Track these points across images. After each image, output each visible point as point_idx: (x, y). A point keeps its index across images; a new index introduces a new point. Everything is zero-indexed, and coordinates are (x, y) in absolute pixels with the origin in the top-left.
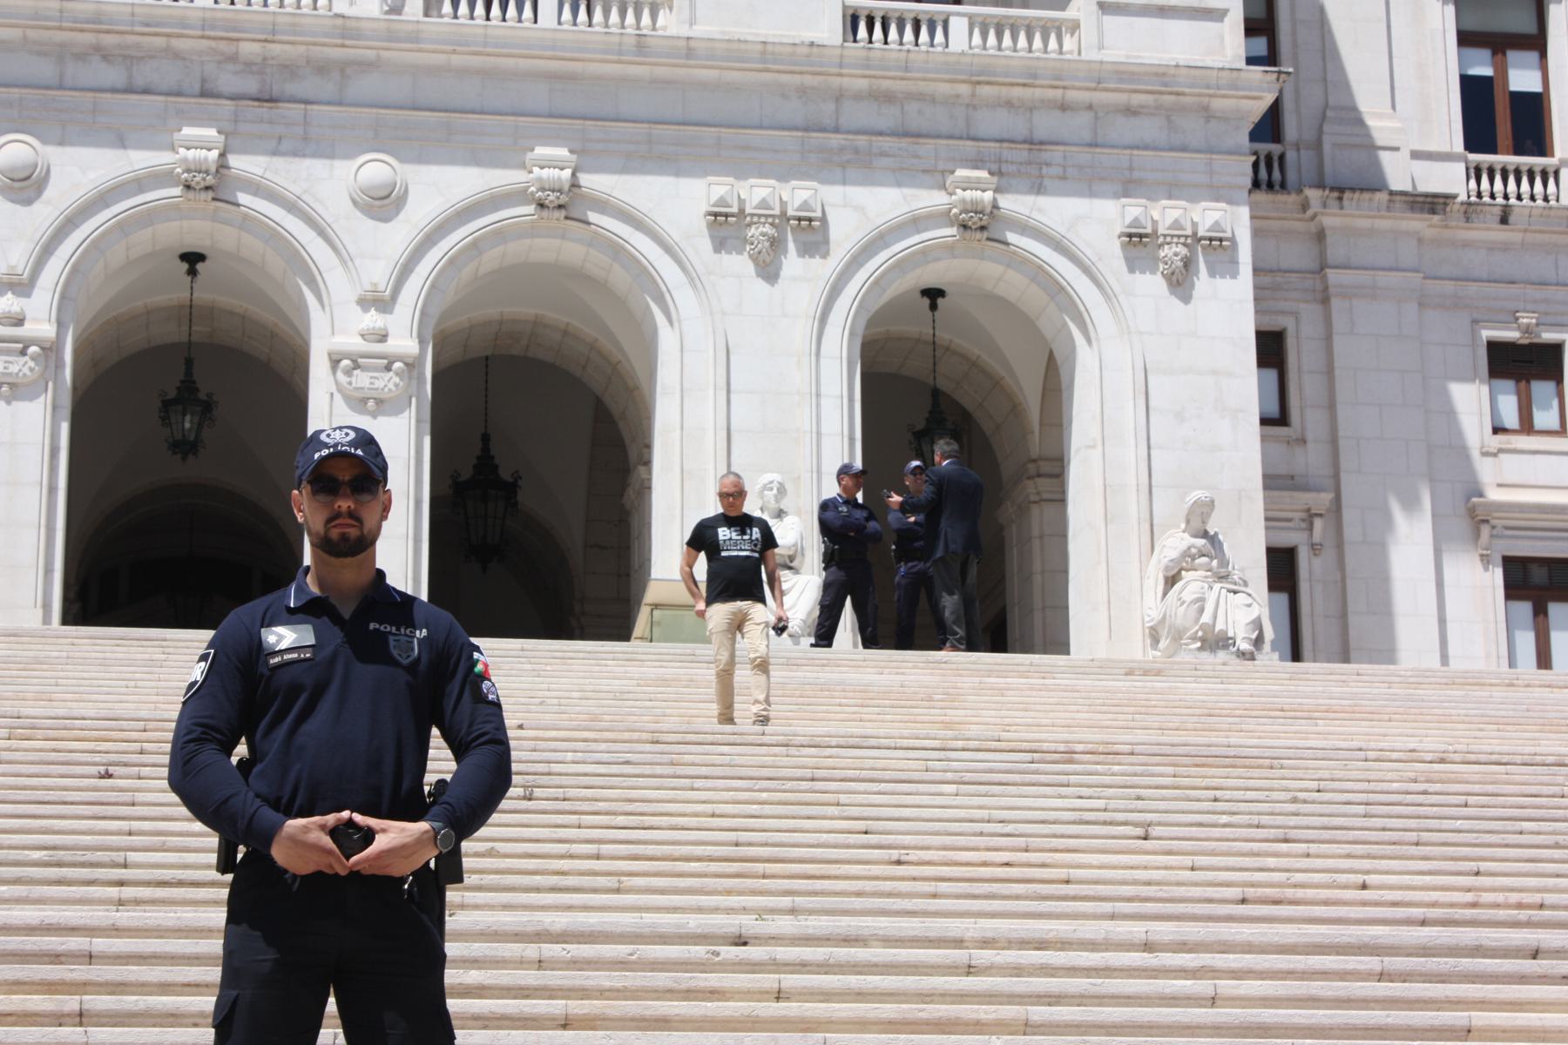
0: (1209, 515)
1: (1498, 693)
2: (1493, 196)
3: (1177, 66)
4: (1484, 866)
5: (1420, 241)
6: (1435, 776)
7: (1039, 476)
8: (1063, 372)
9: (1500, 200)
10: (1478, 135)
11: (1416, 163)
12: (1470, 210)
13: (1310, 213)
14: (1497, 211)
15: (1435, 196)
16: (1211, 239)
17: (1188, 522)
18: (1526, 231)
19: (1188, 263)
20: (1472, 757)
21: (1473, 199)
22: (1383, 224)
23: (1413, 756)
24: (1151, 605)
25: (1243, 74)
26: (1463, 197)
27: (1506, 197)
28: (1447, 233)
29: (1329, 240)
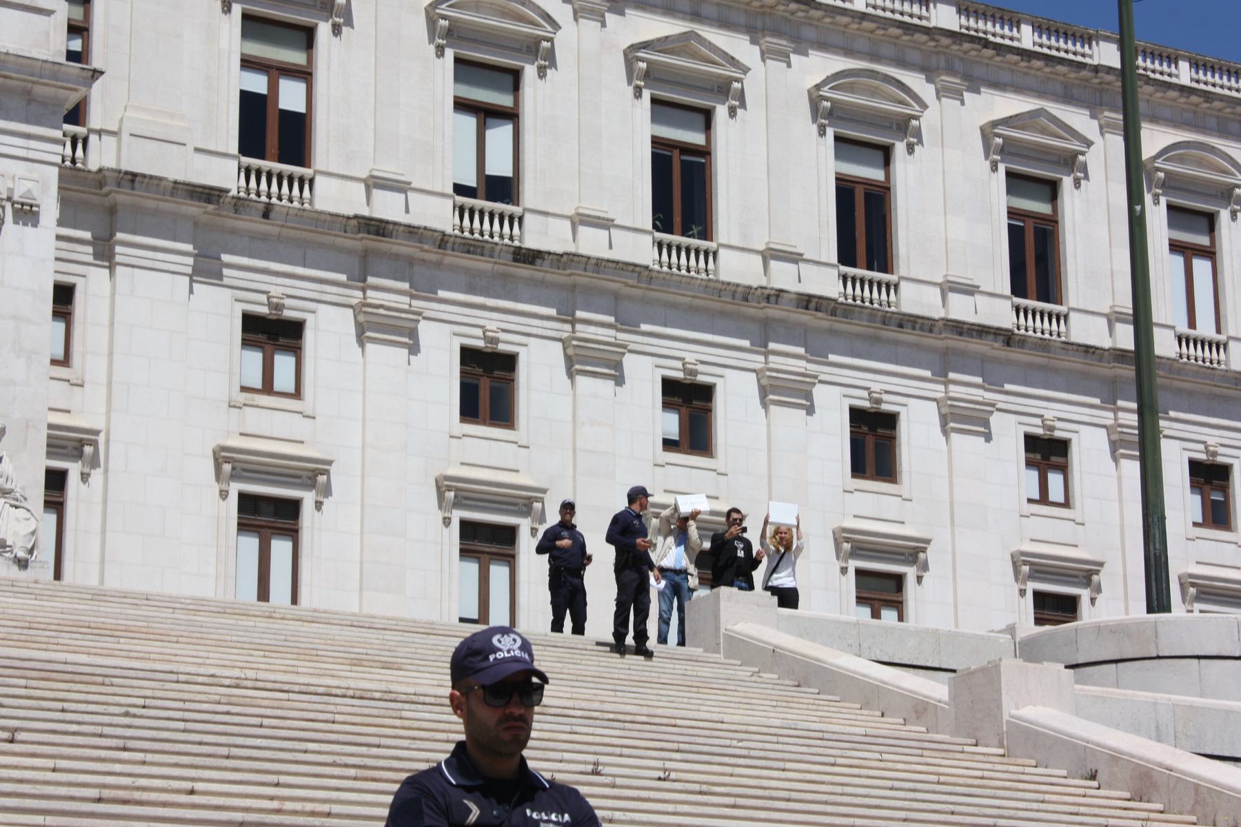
2: (258, 195)
3: (7, 54)
9: (264, 199)
10: (251, 142)
12: (239, 204)
13: (106, 189)
14: (261, 207)
15: (212, 188)
16: (23, 204)
18: (282, 226)
20: (261, 684)
21: (242, 194)
22: (164, 206)
25: (63, 69)
26: (234, 192)
27: (269, 196)
28: (218, 220)
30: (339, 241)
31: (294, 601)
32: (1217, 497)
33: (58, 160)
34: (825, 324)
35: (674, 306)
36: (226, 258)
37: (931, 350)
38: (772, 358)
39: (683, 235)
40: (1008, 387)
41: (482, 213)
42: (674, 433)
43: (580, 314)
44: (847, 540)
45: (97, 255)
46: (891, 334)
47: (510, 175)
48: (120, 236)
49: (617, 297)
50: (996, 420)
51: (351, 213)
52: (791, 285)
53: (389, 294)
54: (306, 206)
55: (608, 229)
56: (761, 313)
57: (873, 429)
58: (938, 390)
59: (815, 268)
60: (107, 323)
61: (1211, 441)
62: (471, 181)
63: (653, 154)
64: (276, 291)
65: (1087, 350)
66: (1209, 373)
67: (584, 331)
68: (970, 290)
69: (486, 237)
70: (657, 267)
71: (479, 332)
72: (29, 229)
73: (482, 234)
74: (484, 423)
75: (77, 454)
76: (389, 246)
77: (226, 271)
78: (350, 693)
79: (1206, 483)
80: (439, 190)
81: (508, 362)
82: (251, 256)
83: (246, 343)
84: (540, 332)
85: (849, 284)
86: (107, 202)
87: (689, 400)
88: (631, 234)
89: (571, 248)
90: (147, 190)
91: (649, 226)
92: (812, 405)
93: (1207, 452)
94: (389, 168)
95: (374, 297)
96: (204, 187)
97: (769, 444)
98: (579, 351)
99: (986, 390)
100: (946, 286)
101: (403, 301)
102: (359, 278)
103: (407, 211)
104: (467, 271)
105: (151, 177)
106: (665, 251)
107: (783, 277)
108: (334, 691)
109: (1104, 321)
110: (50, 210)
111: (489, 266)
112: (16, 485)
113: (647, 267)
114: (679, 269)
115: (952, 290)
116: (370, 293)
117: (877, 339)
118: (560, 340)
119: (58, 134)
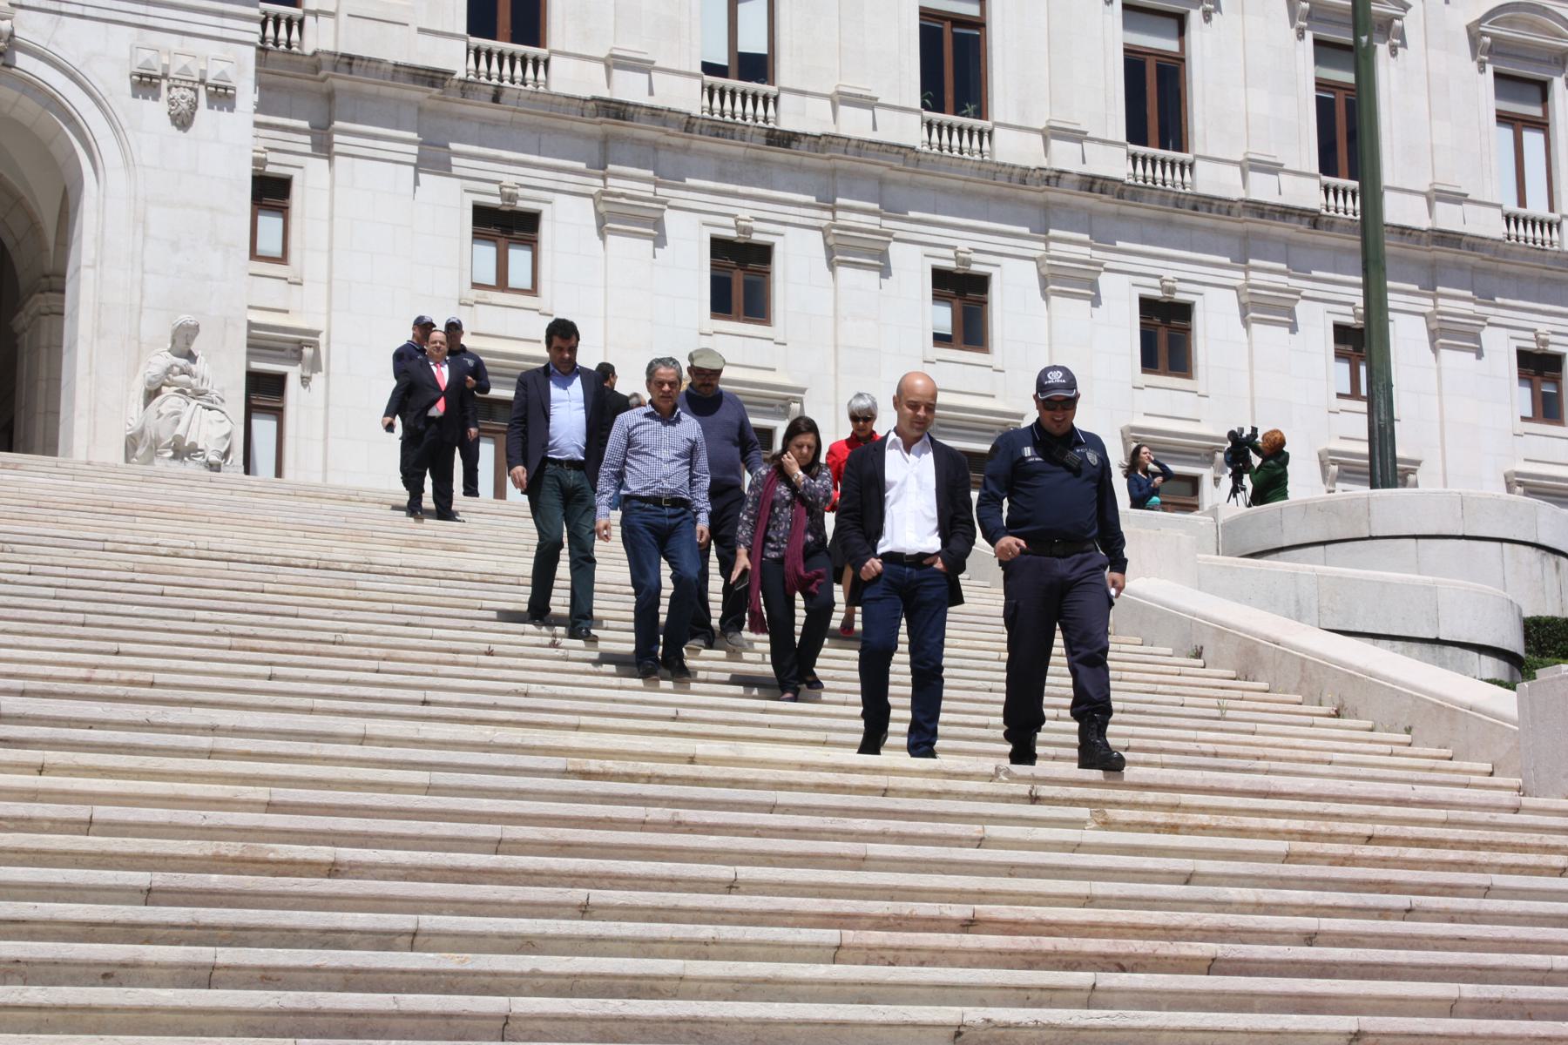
0: (193, 338)
2: (489, 77)
4: (123, 647)
5: (420, 110)
6: (152, 568)
7: (51, 291)
8: (71, 195)
9: (495, 81)
11: (422, 36)
12: (466, 87)
13: (322, 74)
14: (490, 90)
15: (436, 71)
17: (173, 342)
19: (194, 106)
23: (153, 550)
24: (134, 414)
26: (461, 74)
27: (501, 79)
29: (338, 100)
30: (577, 126)
33: (256, 39)
34: (1112, 208)
35: (945, 190)
36: (454, 146)
38: (1052, 245)
39: (956, 113)
41: (733, 93)
42: (946, 327)
43: (840, 201)
45: (313, 144)
46: (1185, 217)
47: (765, 52)
48: (338, 124)
49: (881, 181)
51: (588, 95)
52: (1076, 167)
53: (632, 183)
54: (541, 89)
55: (872, 108)
56: (1040, 197)
59: (1101, 147)
60: (327, 217)
62: (722, 59)
63: (921, 26)
64: (508, 180)
67: (845, 218)
69: (738, 119)
70: (926, 149)
72: (225, 114)
73: (733, 116)
74: (738, 320)
75: (298, 357)
76: (630, 130)
77: (454, 160)
78: (314, 563)
79: (1537, 374)
80: (687, 69)
81: (763, 253)
82: (480, 145)
83: (477, 237)
86: (325, 87)
87: (963, 291)
88: (897, 114)
89: (831, 129)
90: (366, 74)
91: (918, 105)
92: (1098, 296)
93: (1537, 340)
94: (631, 47)
95: (615, 185)
96: (428, 70)
97: (1050, 338)
98: (840, 240)
99: (1291, 276)
100: (1246, 165)
101: (646, 189)
102: (600, 166)
103: (651, 93)
104: (718, 156)
105: (370, 60)
106: (935, 131)
107: (1065, 157)
108: (293, 561)
109: (1423, 200)
110: (247, 95)
111: (740, 151)
113: (913, 149)
114: (951, 150)
115: (1254, 169)
116: (610, 181)
117: (1169, 223)
118: (820, 229)
119: (255, 12)
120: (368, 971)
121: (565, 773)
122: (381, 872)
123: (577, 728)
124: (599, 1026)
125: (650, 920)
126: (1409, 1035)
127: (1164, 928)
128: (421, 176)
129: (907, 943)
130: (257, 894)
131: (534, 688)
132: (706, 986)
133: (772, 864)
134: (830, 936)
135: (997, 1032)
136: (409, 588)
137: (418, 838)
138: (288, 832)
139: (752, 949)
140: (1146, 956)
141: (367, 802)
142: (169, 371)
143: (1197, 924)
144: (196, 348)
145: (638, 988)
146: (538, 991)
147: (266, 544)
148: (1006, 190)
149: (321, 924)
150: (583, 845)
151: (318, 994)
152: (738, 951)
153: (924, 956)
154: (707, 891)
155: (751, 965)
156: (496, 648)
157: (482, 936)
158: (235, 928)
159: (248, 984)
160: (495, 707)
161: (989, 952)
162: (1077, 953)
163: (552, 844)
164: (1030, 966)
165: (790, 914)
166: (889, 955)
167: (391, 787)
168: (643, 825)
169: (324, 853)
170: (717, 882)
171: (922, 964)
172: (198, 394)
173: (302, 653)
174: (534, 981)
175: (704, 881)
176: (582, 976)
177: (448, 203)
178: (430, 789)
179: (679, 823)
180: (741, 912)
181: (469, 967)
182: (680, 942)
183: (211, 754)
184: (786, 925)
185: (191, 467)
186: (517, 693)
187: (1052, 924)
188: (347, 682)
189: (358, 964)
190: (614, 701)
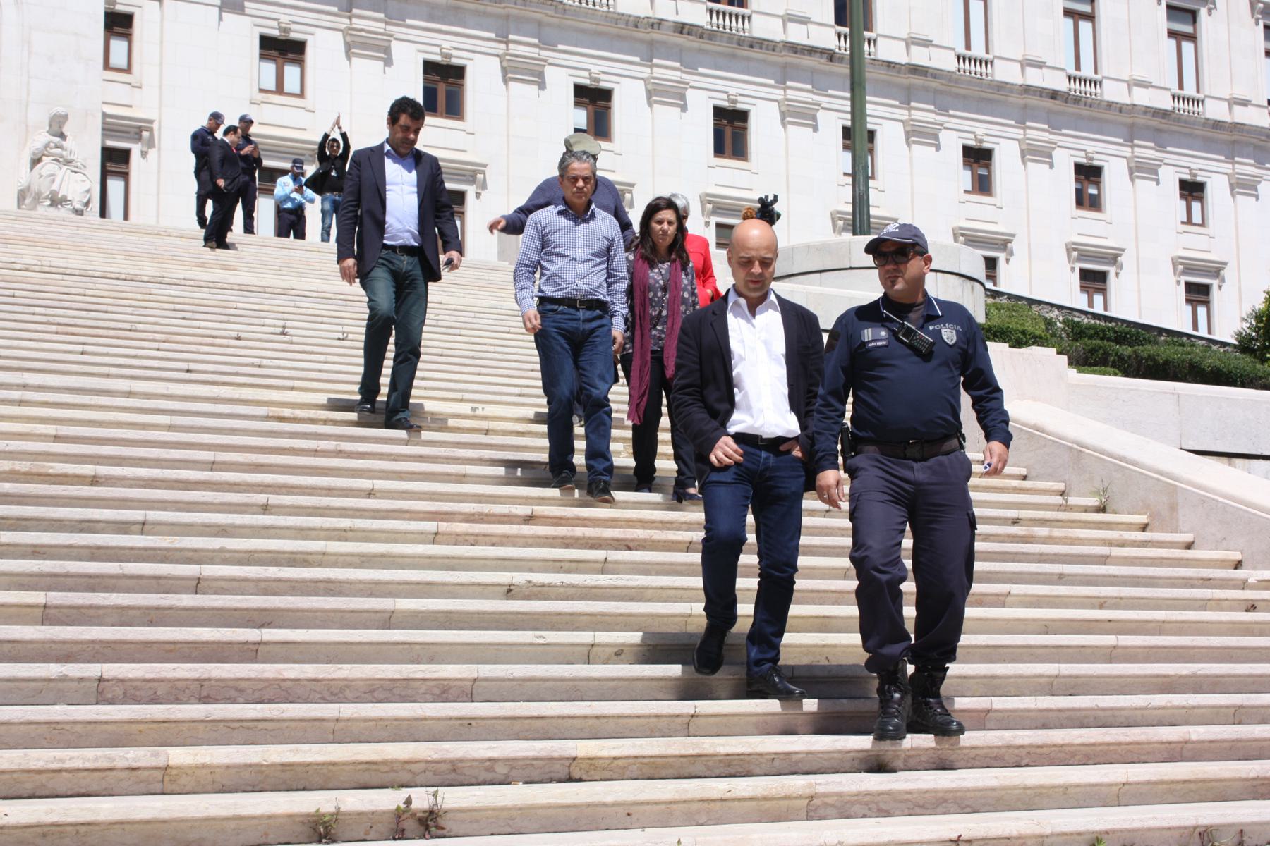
0: (64, 123)
1: (145, 238)
17: (50, 126)
24: (23, 176)
31: (126, 217)
32: (983, 172)
37: (774, 64)
38: (655, 70)
40: (830, 92)
42: (583, 124)
43: (511, 37)
44: (710, 202)
49: (540, 24)
50: (821, 115)
57: (731, 122)
58: (779, 94)
61: (979, 132)
64: (284, 19)
65: (889, 64)
66: (978, 81)
68: (804, 21)
71: (437, 50)
74: (441, 116)
75: (138, 138)
83: (263, 57)
84: (483, 50)
85: (715, 16)
87: (594, 98)
92: (685, 104)
95: (357, 23)
112: (78, 157)
116: (354, 20)
120: (107, 548)
121: (268, 418)
122: (128, 482)
123: (292, 389)
124: (263, 585)
125: (310, 515)
126: (813, 591)
127: (661, 522)
128: (224, 14)
129: (483, 531)
130: (37, 497)
131: (265, 362)
132: (341, 559)
133: (402, 479)
134: (431, 526)
135: (535, 589)
136: (188, 294)
137: (157, 460)
138: (65, 455)
139: (377, 535)
140: (645, 540)
141: (124, 436)
142: (47, 146)
143: (683, 519)
144: (65, 130)
145: (294, 560)
146: (225, 562)
147: (95, 263)
148: (624, 32)
149: (78, 517)
150: (271, 465)
151: (67, 563)
152: (367, 536)
153: (495, 540)
154: (353, 497)
155: (372, 545)
156: (242, 335)
157: (191, 525)
158: (18, 519)
159: (23, 556)
160: (237, 374)
161: (539, 537)
162: (599, 538)
163: (250, 465)
164: (567, 546)
165: (407, 512)
166: (471, 539)
167: (144, 426)
168: (315, 453)
169: (87, 469)
170: (360, 490)
171: (493, 545)
172: (68, 162)
173: (107, 337)
174: (222, 555)
175: (351, 490)
176: (256, 552)
177: (242, 34)
178: (170, 428)
179: (340, 452)
180: (373, 510)
181: (177, 545)
182: (328, 530)
183: (21, 403)
184: (404, 519)
185: (62, 212)
186: (253, 365)
187: (585, 519)
188: (135, 357)
189: (99, 543)
190: (320, 371)
